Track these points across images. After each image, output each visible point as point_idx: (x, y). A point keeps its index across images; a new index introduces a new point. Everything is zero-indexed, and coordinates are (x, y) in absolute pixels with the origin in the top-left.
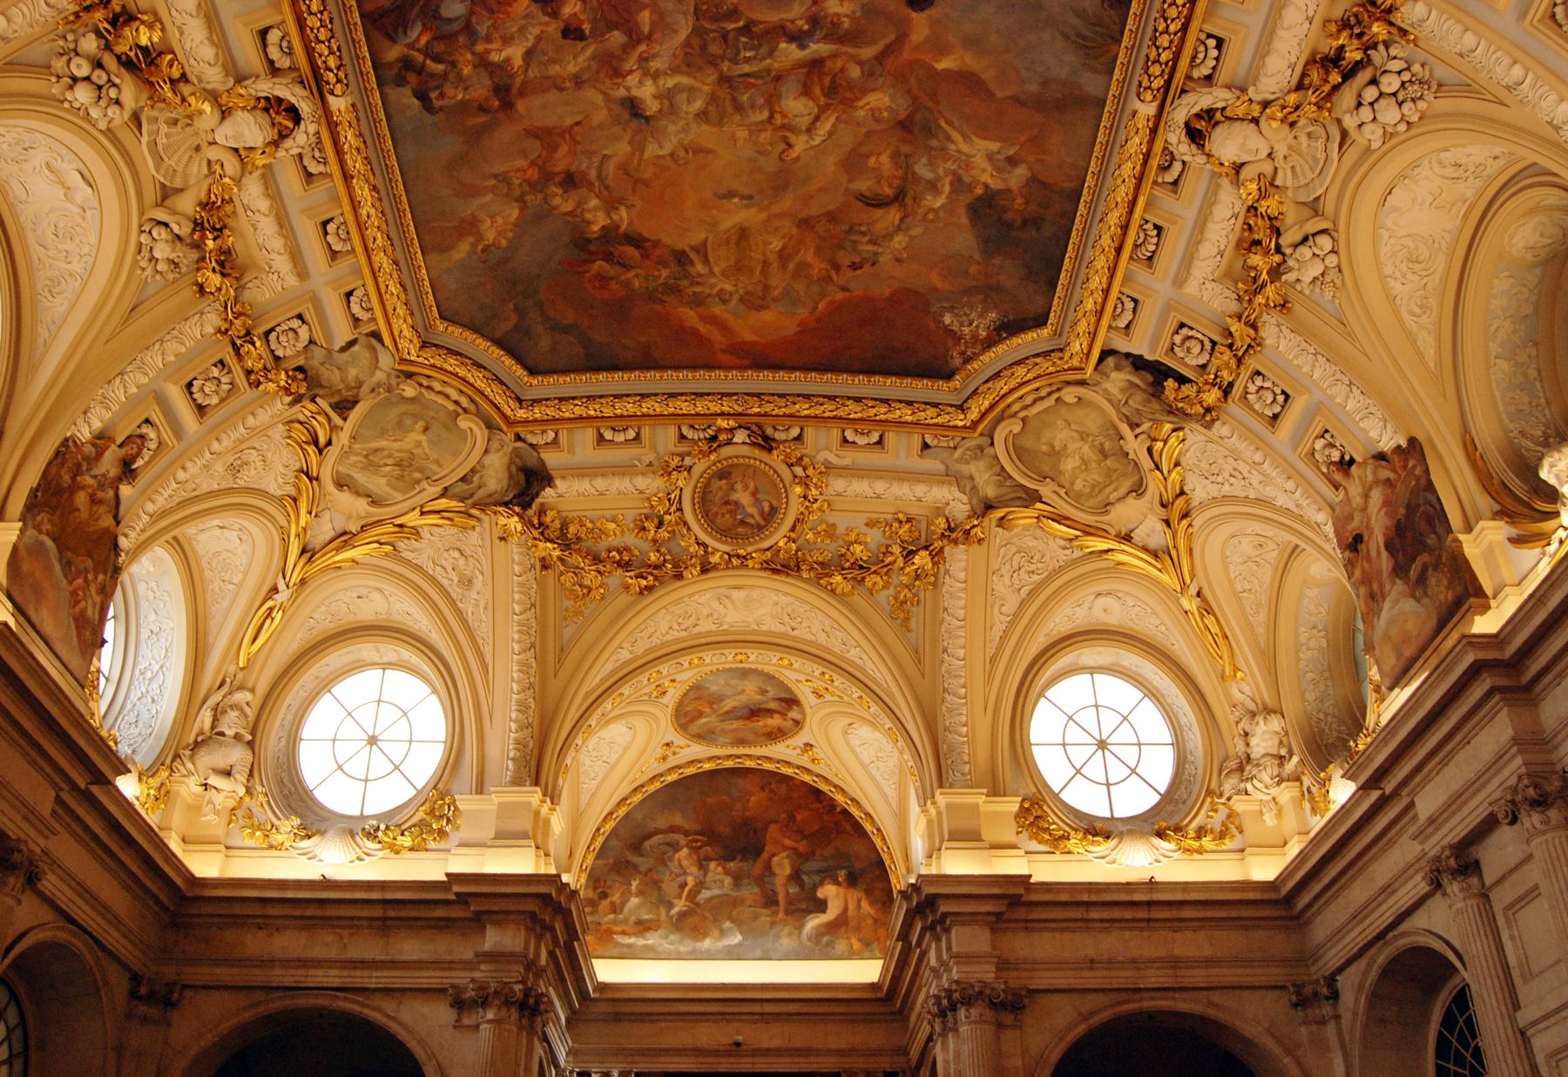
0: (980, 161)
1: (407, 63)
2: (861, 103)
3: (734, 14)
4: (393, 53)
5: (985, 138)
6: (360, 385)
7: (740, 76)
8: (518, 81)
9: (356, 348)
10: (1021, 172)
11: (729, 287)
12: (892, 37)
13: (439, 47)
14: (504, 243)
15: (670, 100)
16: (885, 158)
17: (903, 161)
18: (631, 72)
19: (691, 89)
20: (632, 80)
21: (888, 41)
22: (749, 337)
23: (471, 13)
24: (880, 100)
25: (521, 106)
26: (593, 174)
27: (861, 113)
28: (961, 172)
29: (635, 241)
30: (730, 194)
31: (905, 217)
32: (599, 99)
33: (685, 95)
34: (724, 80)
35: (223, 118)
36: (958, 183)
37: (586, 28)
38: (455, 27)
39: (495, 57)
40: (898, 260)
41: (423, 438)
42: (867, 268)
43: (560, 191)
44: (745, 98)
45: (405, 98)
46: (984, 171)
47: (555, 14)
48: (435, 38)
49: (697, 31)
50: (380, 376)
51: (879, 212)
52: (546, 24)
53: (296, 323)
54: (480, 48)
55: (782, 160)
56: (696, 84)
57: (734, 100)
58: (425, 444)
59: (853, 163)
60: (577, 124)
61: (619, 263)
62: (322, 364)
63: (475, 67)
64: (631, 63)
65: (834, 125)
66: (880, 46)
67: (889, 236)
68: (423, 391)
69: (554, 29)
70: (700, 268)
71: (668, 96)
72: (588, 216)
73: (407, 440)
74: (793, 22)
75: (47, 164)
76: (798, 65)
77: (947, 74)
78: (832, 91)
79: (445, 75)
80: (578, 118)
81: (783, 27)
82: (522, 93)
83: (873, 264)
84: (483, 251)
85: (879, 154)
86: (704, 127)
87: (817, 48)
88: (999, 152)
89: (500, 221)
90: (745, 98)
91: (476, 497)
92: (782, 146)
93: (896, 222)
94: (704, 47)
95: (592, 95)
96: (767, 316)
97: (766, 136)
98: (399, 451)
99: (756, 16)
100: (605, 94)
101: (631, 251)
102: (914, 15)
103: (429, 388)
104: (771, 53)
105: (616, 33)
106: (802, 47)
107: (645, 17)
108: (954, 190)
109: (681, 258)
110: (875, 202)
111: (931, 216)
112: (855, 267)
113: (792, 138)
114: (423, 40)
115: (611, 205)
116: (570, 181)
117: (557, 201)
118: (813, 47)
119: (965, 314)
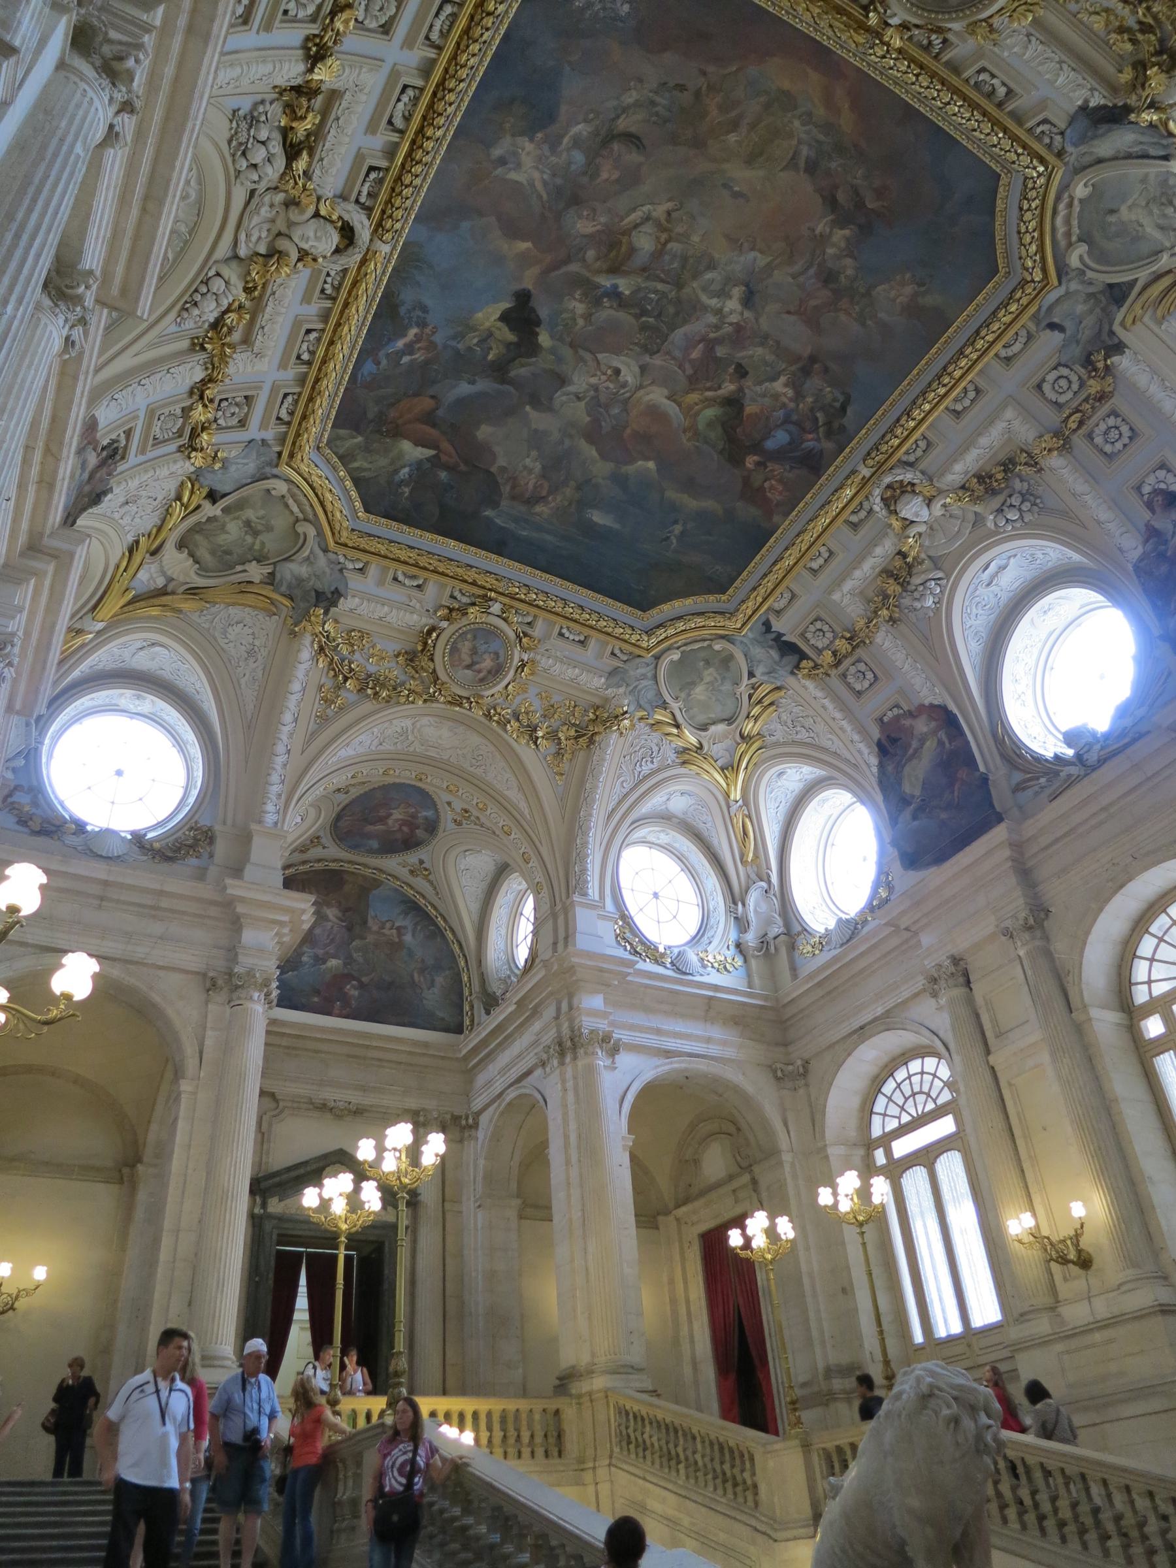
0: (527, 161)
1: (829, 434)
2: (599, 227)
3: (644, 328)
4: (828, 446)
5: (517, 182)
6: (1091, 296)
7: (668, 283)
8: (793, 368)
9: (1056, 320)
10: (497, 152)
11: (797, 123)
12: (553, 274)
13: (808, 425)
14: (908, 276)
15: (723, 289)
16: (604, 175)
17: (591, 170)
18: (731, 324)
19: (704, 289)
20: (734, 319)
21: (557, 273)
22: (814, 76)
23: (778, 426)
24: (583, 226)
25: (807, 352)
26: (812, 271)
27: (603, 220)
28: (547, 153)
29: (831, 202)
30: (737, 195)
31: (613, 120)
32: (763, 321)
33: (712, 288)
34: (679, 285)
35: (913, 522)
36: (554, 144)
37: (731, 370)
38: (792, 428)
39: (790, 393)
40: (640, 80)
41: (1124, 210)
42: (671, 84)
43: (842, 276)
44: (675, 265)
45: (849, 419)
46: (528, 154)
47: (741, 389)
48: (803, 430)
49: (673, 327)
50: (1074, 286)
51: (633, 129)
52: (749, 387)
53: (1046, 387)
54: (792, 405)
55: (681, 204)
56: (699, 292)
57: (683, 267)
58: (1130, 202)
59: (631, 179)
60: (789, 313)
61: (858, 194)
62: (1078, 342)
63: (804, 397)
64: (727, 329)
65: (628, 215)
66: (564, 269)
67: (637, 104)
68: (1074, 238)
69: (748, 382)
70: (805, 151)
71: (723, 294)
72: (843, 245)
73: (1133, 217)
74: (611, 307)
75: (988, 585)
76: (625, 274)
77: (524, 240)
78: (614, 245)
79: (822, 409)
80: (785, 316)
81: (620, 305)
82: (799, 358)
83: (665, 84)
84: (923, 285)
85: (607, 180)
86: (717, 256)
87: (606, 282)
88: (510, 170)
89: (893, 293)
90: (675, 265)
91: (1155, 140)
92: (674, 215)
93: (624, 116)
94: (677, 314)
95: (764, 324)
96: (786, 85)
97: (679, 229)
98: (1151, 213)
99: (632, 320)
100: (757, 320)
101: (841, 197)
102: (530, 287)
103: (1068, 234)
104: (639, 290)
105: (718, 355)
106: (615, 286)
107: (695, 354)
108: (563, 136)
109: (811, 168)
110: (632, 139)
111: (591, 116)
112: (681, 88)
113: (663, 219)
114: (810, 436)
115: (822, 240)
116: (829, 277)
117: (849, 272)
118: (608, 284)
119: (604, 9)
